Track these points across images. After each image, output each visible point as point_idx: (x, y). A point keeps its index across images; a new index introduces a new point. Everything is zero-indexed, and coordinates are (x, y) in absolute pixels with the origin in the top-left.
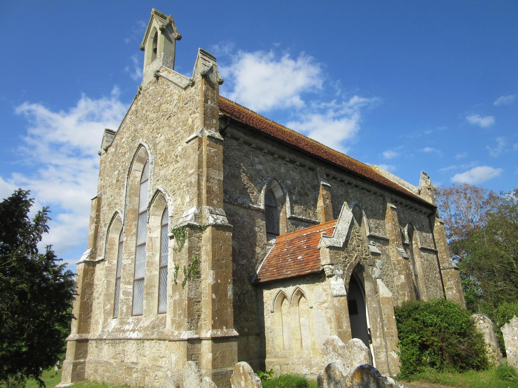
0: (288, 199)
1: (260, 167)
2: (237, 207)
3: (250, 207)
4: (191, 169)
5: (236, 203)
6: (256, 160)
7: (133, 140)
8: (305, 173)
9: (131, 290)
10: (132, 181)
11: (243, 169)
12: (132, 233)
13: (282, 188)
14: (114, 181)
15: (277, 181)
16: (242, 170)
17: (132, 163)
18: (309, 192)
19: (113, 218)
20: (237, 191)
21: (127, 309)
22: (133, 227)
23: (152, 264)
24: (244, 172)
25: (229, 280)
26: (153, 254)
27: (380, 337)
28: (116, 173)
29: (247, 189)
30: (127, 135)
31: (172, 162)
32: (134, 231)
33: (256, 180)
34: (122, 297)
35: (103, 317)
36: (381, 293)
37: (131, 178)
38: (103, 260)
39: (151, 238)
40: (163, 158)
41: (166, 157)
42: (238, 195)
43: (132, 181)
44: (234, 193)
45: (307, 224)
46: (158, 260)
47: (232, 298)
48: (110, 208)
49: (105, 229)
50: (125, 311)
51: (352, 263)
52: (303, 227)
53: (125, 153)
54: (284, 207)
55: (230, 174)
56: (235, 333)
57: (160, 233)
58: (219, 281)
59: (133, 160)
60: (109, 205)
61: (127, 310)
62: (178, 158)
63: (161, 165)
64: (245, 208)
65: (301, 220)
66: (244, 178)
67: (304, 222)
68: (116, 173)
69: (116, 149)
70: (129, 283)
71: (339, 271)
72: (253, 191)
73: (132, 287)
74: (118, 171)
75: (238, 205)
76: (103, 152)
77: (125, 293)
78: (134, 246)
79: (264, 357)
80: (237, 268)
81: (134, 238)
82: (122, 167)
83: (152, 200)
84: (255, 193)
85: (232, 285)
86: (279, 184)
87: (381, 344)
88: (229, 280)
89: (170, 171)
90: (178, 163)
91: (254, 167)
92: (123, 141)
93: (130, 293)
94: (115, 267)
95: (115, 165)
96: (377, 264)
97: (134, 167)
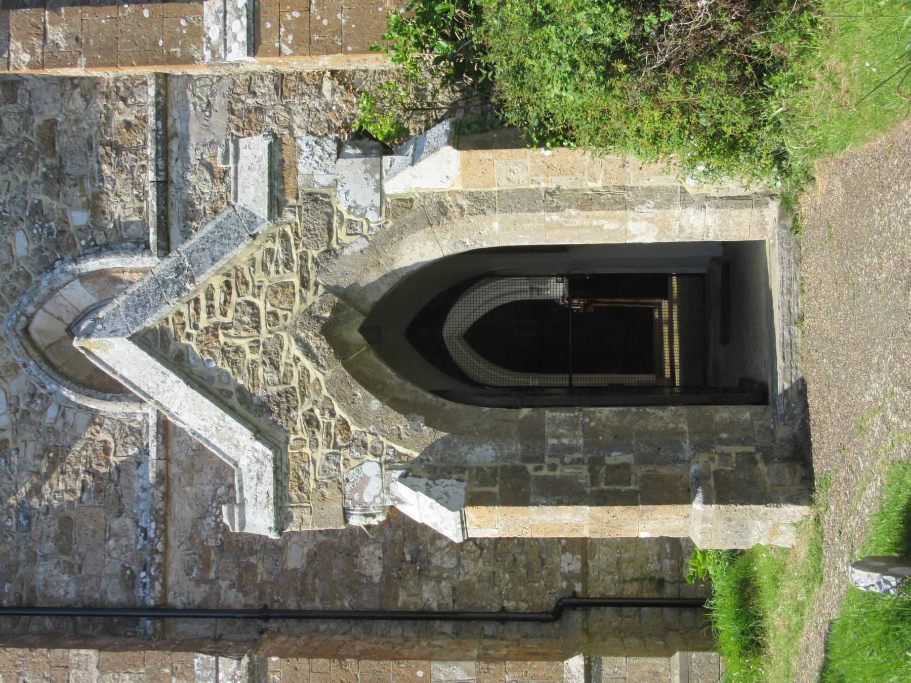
0: (92, 265)
2: (172, 530)
3: (163, 478)
5: (160, 547)
11: (29, 495)
13: (53, 292)
15: (30, 318)
16: (35, 502)
18: (38, 120)
20: (115, 525)
24: (36, 491)
25: (420, 674)
27: (623, 220)
29: (94, 474)
33: (51, 430)
36: (446, 186)
42: (129, 522)
44: (124, 542)
45: (174, 146)
47: (471, 665)
51: (330, 383)
52: (191, 177)
54: (126, 276)
55: (63, 558)
64: (166, 496)
65: (163, 185)
66: (61, 489)
67: (166, 169)
71: (365, 479)
72: (99, 446)
75: (165, 531)
80: (376, 541)
84: (103, 436)
85: (435, 665)
86: (40, 305)
87: (651, 220)
88: (420, 674)
96: (322, 180)
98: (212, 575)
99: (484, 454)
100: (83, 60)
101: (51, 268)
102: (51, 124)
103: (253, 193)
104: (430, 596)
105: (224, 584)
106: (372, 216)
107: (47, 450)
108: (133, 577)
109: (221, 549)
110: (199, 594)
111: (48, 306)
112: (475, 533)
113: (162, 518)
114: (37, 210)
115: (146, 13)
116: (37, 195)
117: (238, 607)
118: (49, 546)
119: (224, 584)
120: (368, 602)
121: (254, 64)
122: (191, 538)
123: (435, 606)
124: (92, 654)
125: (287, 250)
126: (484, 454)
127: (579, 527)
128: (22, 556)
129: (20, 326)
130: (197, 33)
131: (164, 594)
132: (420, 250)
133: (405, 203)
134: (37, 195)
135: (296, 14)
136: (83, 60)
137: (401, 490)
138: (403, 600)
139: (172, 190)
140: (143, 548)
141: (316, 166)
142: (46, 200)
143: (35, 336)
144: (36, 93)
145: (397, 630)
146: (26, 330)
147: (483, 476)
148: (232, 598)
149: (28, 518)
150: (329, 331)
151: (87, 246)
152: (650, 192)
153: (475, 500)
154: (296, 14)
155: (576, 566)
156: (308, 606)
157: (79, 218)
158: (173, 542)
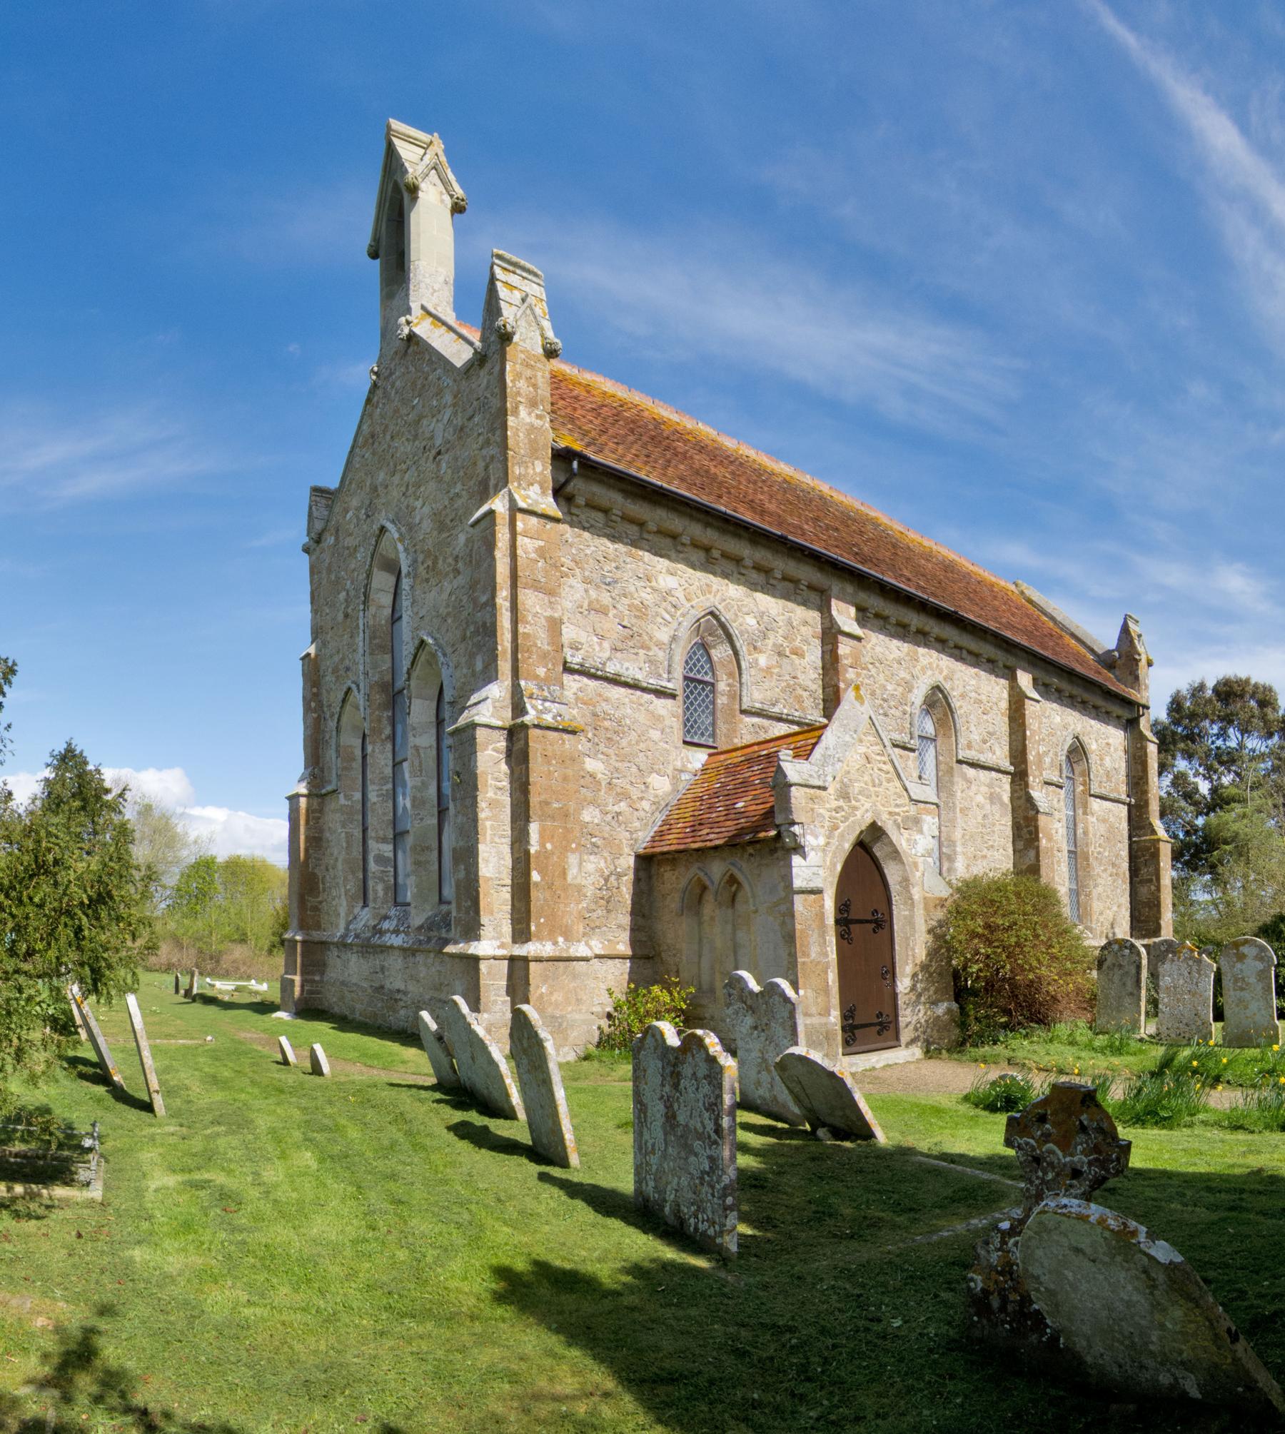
4: (484, 593)
7: (368, 516)
9: (391, 855)
10: (374, 616)
12: (383, 736)
14: (340, 617)
17: (369, 575)
19: (344, 701)
21: (386, 889)
22: (385, 722)
23: (423, 803)
26: (423, 783)
28: (343, 595)
30: (355, 502)
31: (447, 574)
32: (388, 731)
34: (373, 866)
35: (345, 903)
37: (372, 609)
38: (334, 791)
39: (417, 748)
40: (430, 563)
41: (435, 562)
43: (374, 616)
46: (435, 794)
48: (337, 678)
49: (332, 724)
50: (381, 893)
53: (355, 550)
57: (434, 738)
59: (371, 565)
60: (335, 671)
61: (386, 894)
62: (460, 565)
63: (427, 580)
68: (343, 595)
69: (337, 539)
70: (384, 840)
73: (391, 847)
74: (344, 594)
76: (313, 545)
77: (380, 859)
78: (391, 763)
79: (508, 986)
81: (389, 746)
82: (352, 583)
83: (413, 664)
89: (445, 596)
90: (460, 577)
92: (348, 517)
93: (388, 859)
94: (359, 806)
95: (338, 578)
97: (375, 585)
108: (578, 649)
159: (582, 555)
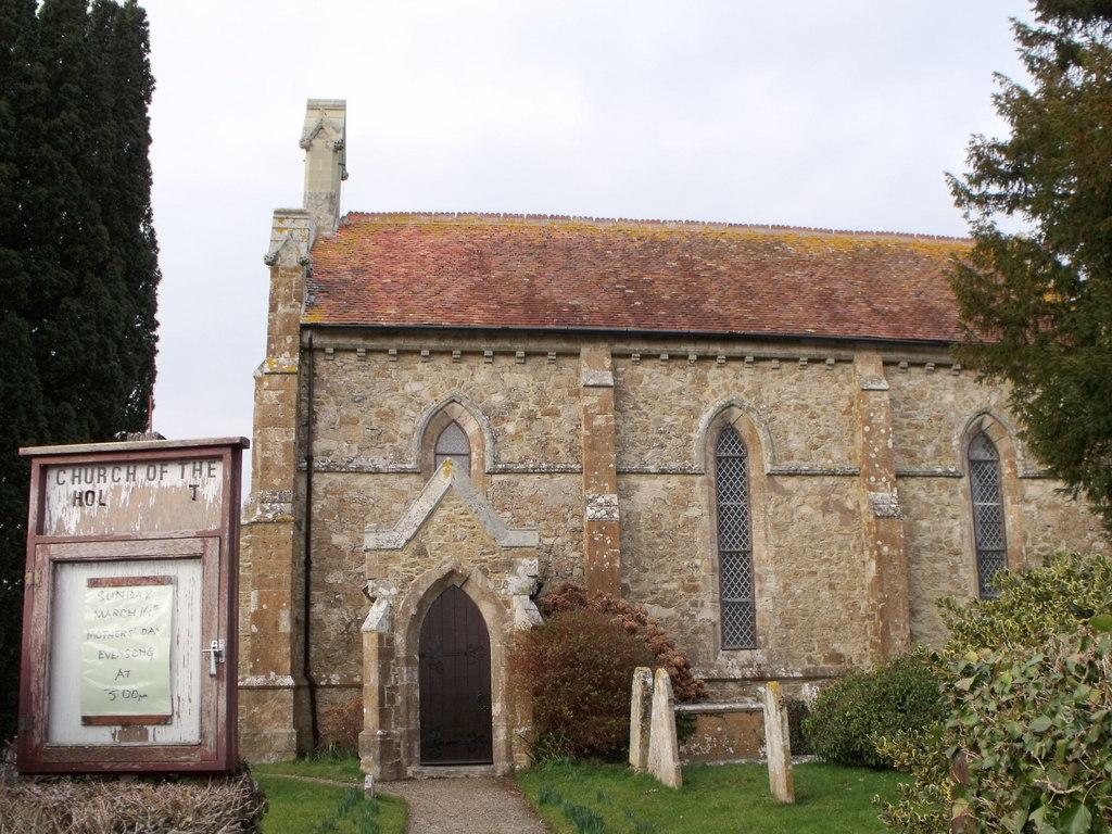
1: (416, 386)
6: (406, 375)
8: (553, 367)
15: (459, 403)
20: (355, 447)
47: (288, 630)
56: (289, 681)
58: (264, 606)
91: (401, 391)
96: (520, 570)
98: (329, 496)
99: (400, 639)
100: (588, 433)
101: (485, 414)
102: (558, 414)
103: (515, 537)
104: (318, 608)
105: (324, 502)
106: (503, 591)
107: (393, 411)
108: (328, 455)
109: (342, 500)
110: (319, 489)
111: (466, 413)
112: (365, 637)
113: (359, 471)
114: (514, 406)
115: (611, 466)
116: (522, 407)
117: (313, 509)
118: (344, 412)
119: (324, 502)
120: (314, 574)
121: (586, 519)
122: (347, 485)
123: (313, 610)
124: (293, 438)
125: (489, 553)
126: (400, 639)
127: (368, 681)
128: (339, 398)
129: (456, 399)
130: (602, 492)
131: (318, 472)
132: (487, 611)
133: (507, 603)
134: (522, 407)
135: (609, 542)
136: (588, 433)
137: (384, 604)
138: (315, 594)
139: (525, 476)
140: (343, 461)
141: (528, 567)
142: (519, 411)
143: (451, 405)
144: (573, 406)
145: (301, 589)
146: (454, 401)
147: (390, 641)
148: (316, 508)
149: (359, 401)
150: (452, 573)
151: (496, 432)
152: (513, 712)
153: (380, 636)
154: (609, 542)
155: (334, 682)
156: (313, 546)
157: (511, 428)
158: (346, 476)
159: (335, 386)
